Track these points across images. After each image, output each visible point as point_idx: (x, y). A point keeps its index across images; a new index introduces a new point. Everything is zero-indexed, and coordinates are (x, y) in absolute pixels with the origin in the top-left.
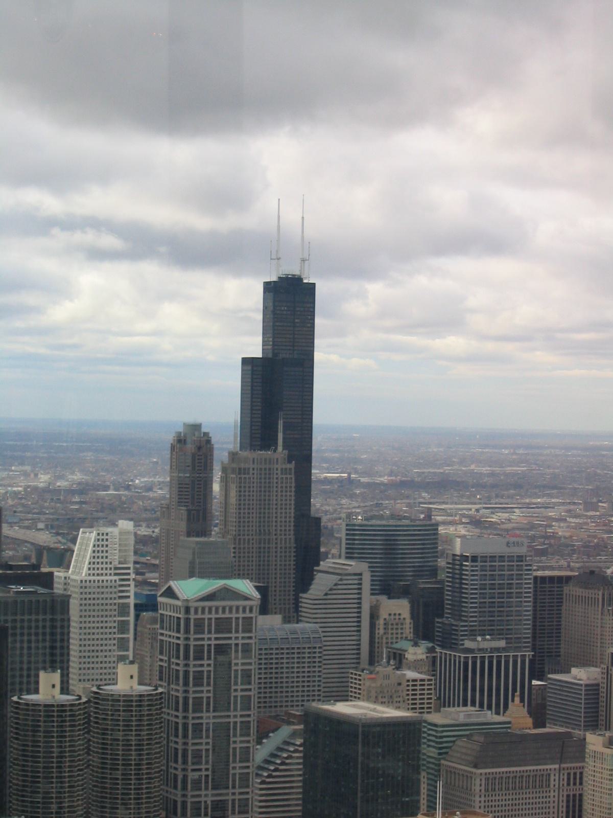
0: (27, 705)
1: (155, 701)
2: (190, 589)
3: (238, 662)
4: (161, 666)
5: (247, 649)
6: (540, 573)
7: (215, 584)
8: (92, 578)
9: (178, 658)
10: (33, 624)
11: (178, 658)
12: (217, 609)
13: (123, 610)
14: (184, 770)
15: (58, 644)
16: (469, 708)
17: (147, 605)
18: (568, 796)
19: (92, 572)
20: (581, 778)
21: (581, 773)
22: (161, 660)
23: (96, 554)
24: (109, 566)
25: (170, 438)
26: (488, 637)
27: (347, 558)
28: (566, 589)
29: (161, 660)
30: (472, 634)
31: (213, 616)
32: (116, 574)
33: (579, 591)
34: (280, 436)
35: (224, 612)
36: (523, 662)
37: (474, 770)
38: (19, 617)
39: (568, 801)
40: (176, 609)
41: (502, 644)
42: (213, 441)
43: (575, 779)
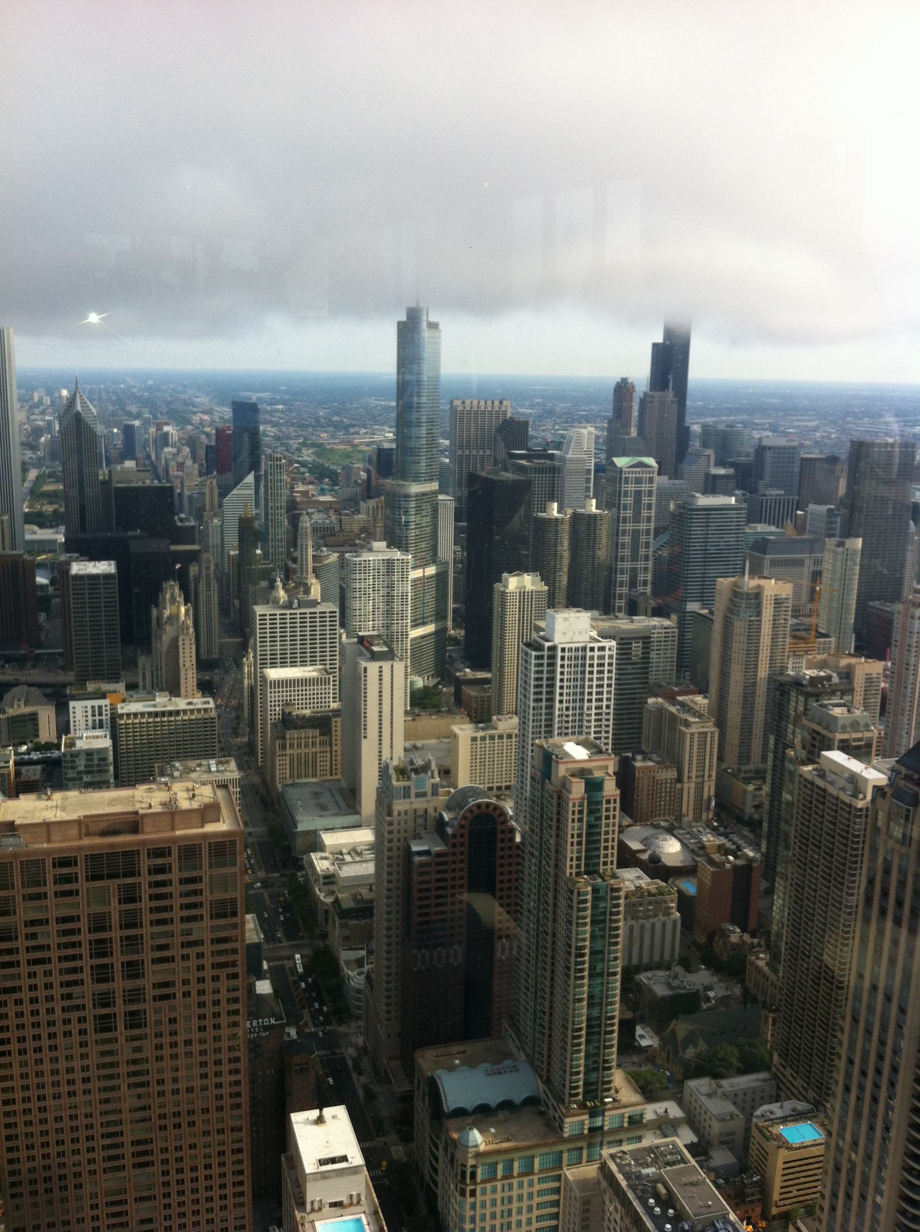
2: (621, 462)
5: (650, 493)
17: (599, 469)
25: (613, 385)
41: (782, 492)
42: (637, 389)
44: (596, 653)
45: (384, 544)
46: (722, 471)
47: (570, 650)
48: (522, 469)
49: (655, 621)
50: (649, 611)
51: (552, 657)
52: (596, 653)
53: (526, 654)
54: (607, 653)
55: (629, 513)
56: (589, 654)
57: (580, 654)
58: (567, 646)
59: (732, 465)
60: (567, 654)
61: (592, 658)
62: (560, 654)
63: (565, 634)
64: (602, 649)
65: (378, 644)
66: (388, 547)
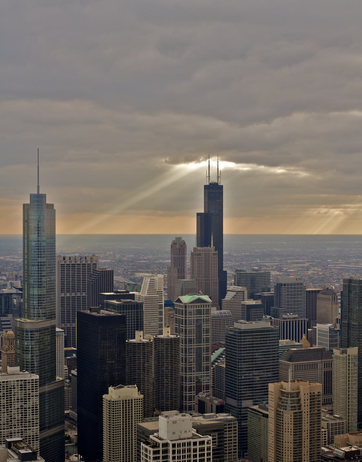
0: (131, 343)
1: (176, 340)
2: (186, 299)
3: (204, 326)
4: (176, 327)
5: (207, 320)
6: (307, 290)
7: (196, 297)
8: (149, 296)
9: (182, 324)
10: (130, 313)
11: (182, 324)
12: (196, 306)
13: (161, 307)
14: (185, 365)
15: (139, 320)
16: (288, 340)
17: (168, 304)
18: (325, 372)
19: (149, 293)
20: (331, 365)
21: (331, 363)
22: (176, 325)
23: (150, 287)
24: (155, 291)
26: (291, 313)
27: (238, 286)
28: (319, 295)
29: (176, 325)
30: (285, 312)
31: (195, 309)
32: (157, 294)
33: (323, 296)
34: (212, 241)
35: (199, 308)
36: (305, 323)
37: (290, 363)
38: (125, 311)
39: (324, 374)
40: (181, 306)
41: (297, 316)
43: (327, 365)
44: (198, 447)
45: (18, 368)
46: (252, 302)
47: (179, 445)
48: (114, 306)
49: (222, 416)
50: (214, 408)
51: (166, 451)
52: (198, 447)
53: (146, 450)
54: (206, 446)
55: (193, 336)
56: (192, 447)
57: (186, 447)
58: (176, 442)
59: (259, 297)
60: (176, 449)
61: (195, 450)
62: (171, 448)
63: (174, 433)
64: (202, 443)
65: (23, 448)
66: (21, 370)
